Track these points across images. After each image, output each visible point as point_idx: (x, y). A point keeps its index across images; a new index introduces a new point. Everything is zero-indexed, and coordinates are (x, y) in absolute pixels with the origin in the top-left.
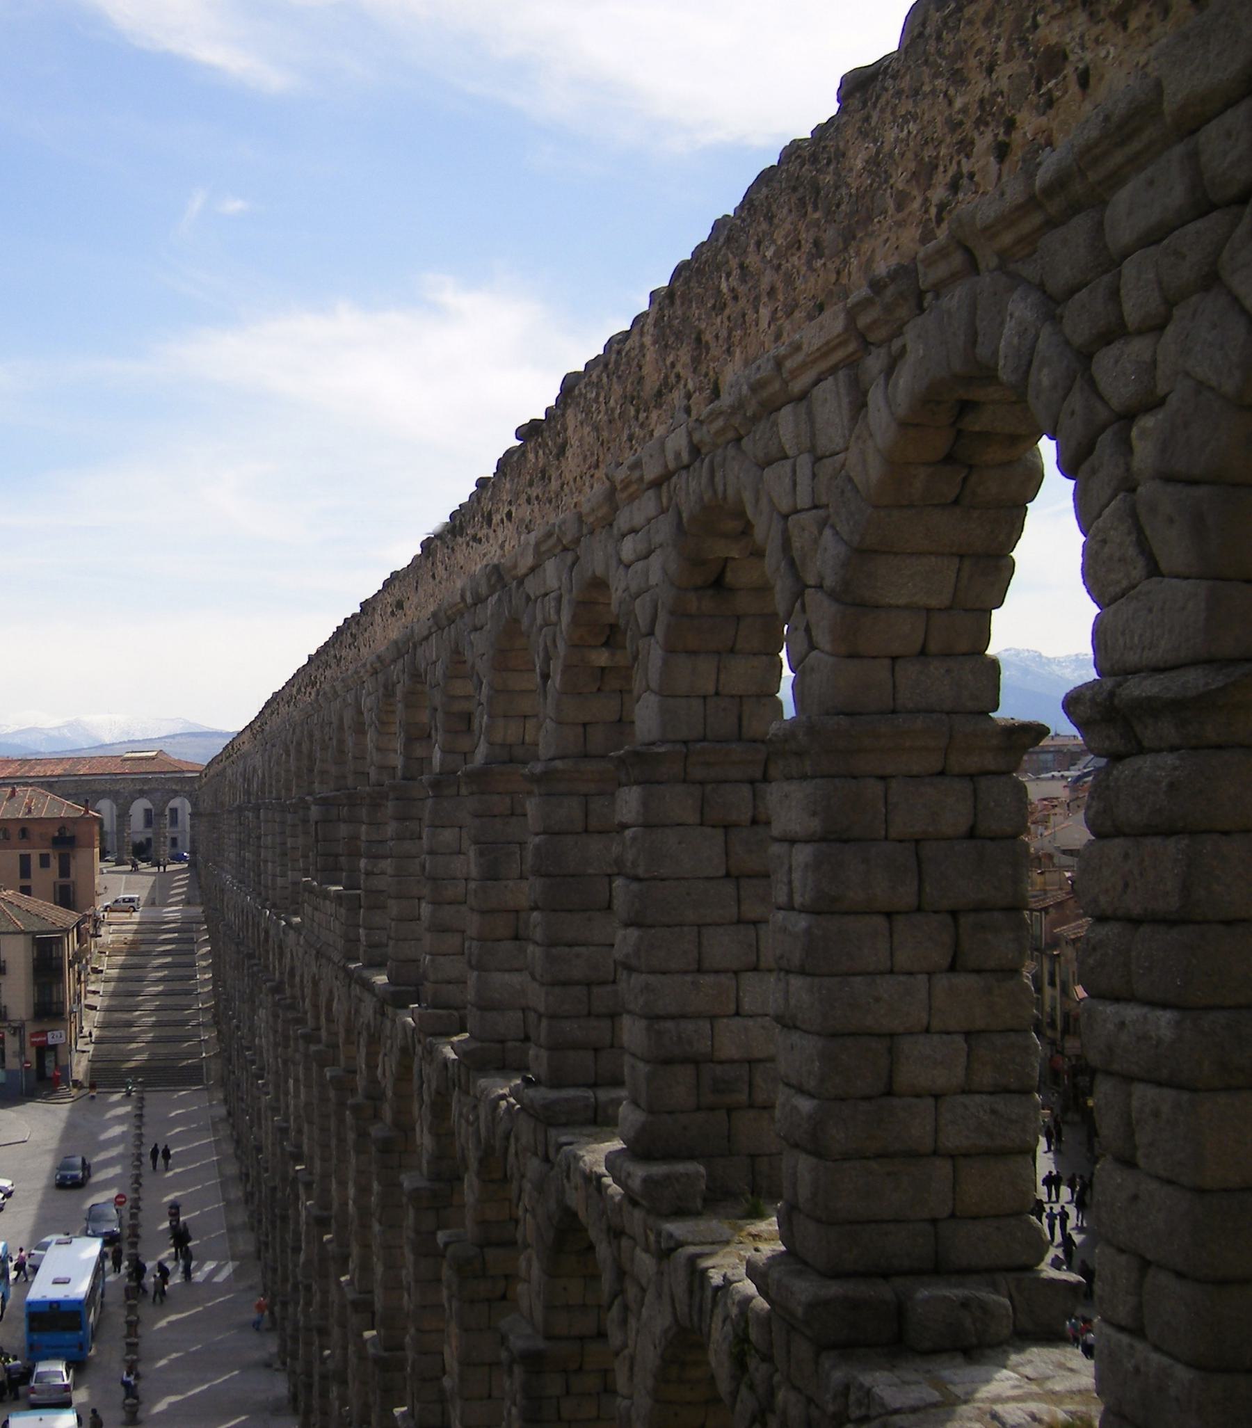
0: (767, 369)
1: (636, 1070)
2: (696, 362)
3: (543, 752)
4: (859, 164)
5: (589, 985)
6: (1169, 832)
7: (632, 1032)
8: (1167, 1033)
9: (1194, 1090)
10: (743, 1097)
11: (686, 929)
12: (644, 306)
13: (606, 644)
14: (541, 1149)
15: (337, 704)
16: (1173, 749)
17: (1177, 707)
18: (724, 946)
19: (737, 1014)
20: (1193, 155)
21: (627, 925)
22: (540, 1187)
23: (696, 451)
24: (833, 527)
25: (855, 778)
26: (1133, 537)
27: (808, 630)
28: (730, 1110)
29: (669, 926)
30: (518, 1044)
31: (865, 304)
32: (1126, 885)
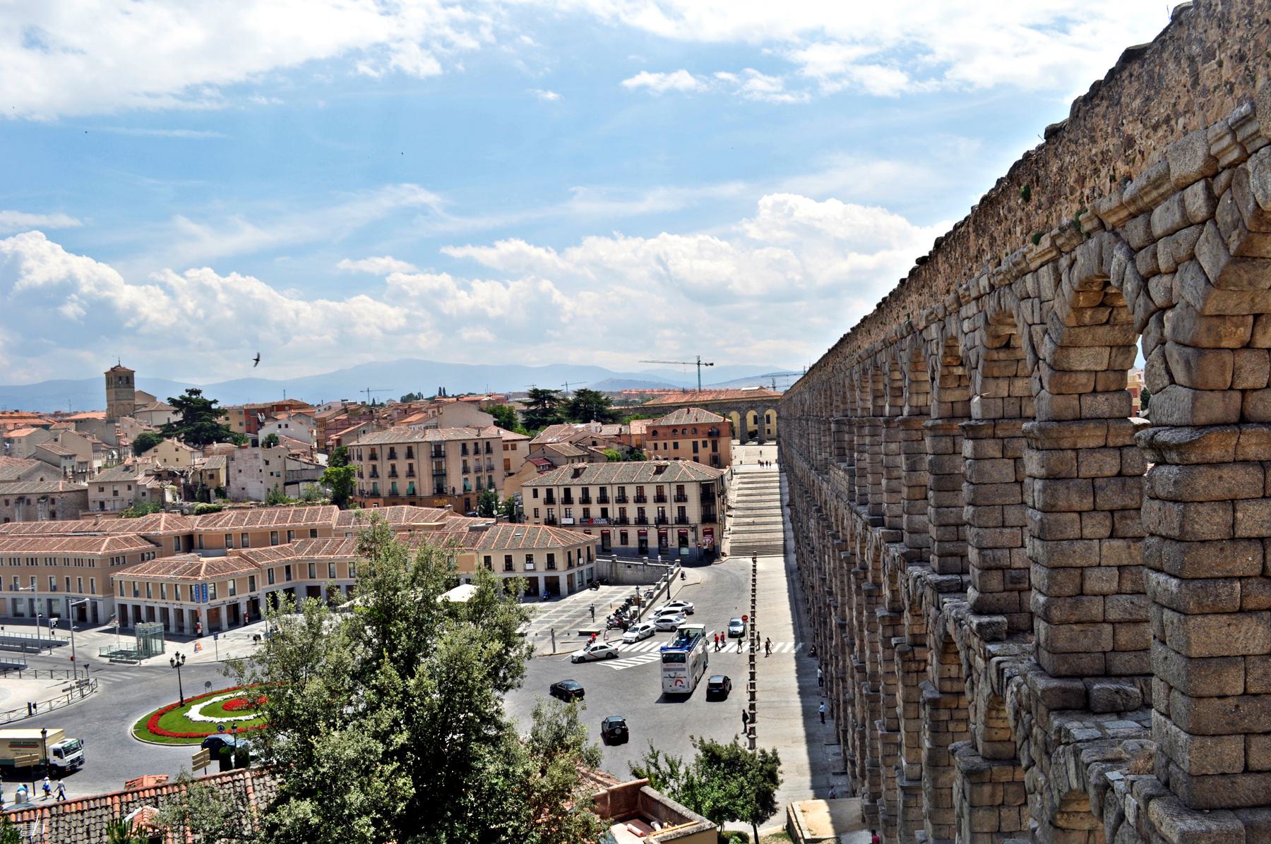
0: (1019, 258)
1: (975, 573)
2: (991, 245)
3: (934, 415)
4: (1055, 170)
6: (1176, 501)
7: (973, 554)
8: (1175, 590)
9: (1186, 615)
12: (969, 212)
15: (842, 375)
16: (1177, 465)
17: (1178, 447)
20: (1182, 201)
21: (969, 504)
22: (935, 621)
23: (992, 287)
28: (1020, 591)
31: (1058, 236)
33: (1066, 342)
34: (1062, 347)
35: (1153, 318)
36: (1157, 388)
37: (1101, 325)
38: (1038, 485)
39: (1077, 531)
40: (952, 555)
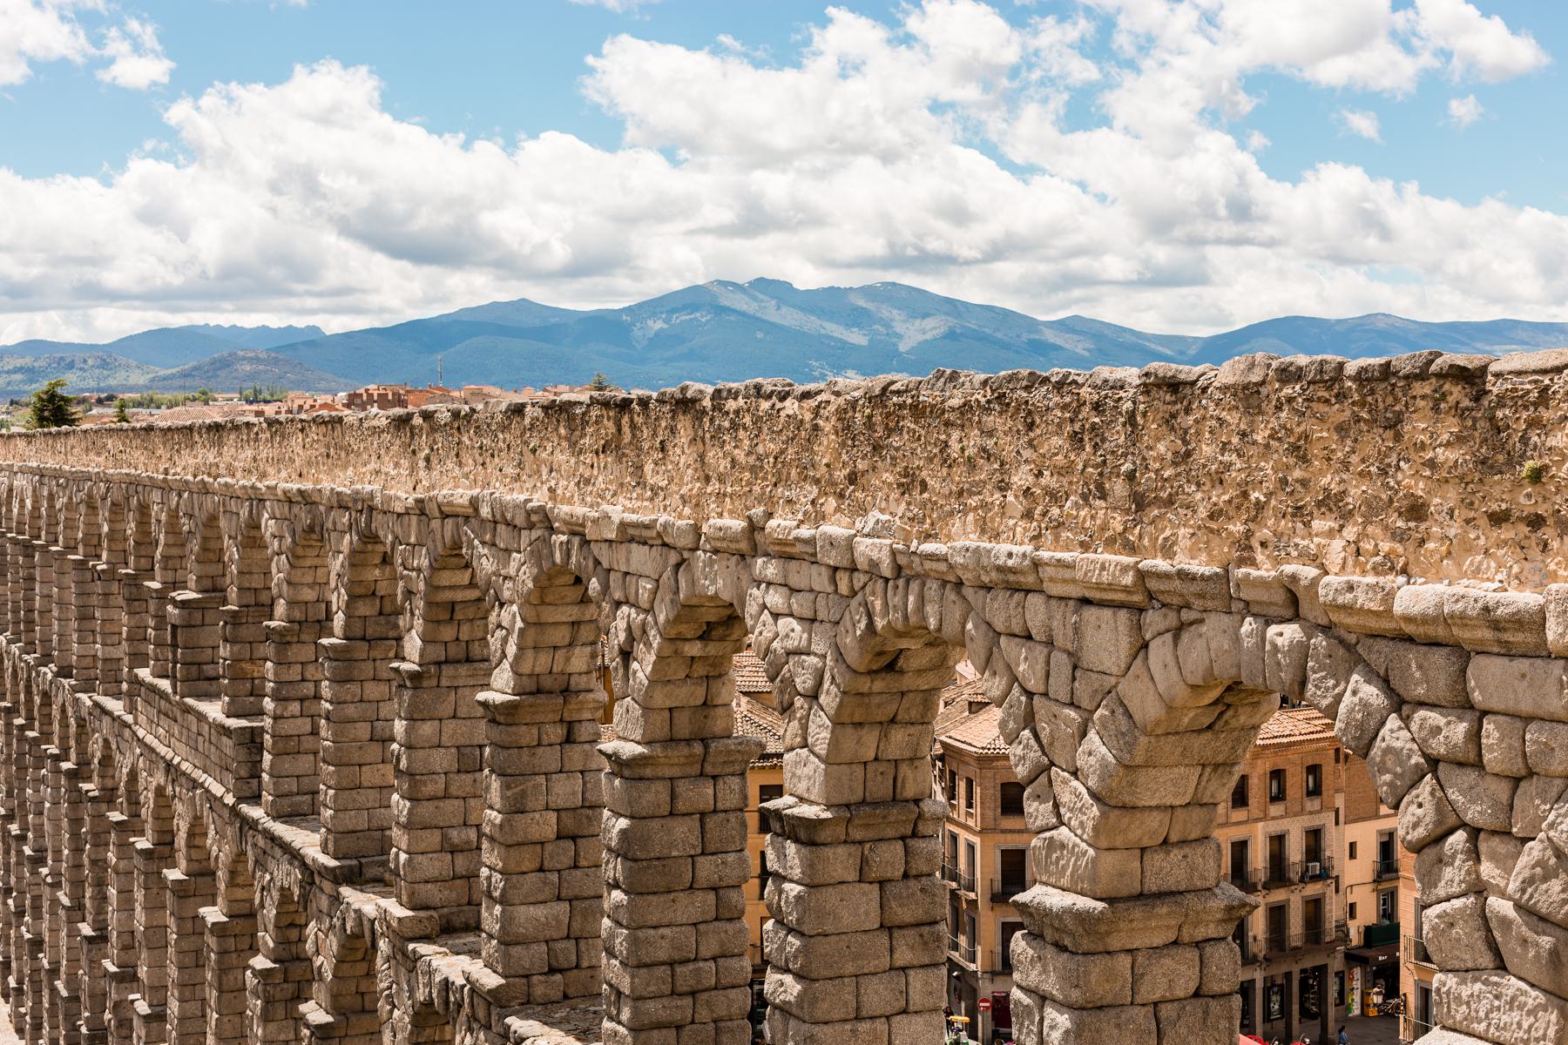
5: (671, 964)
13: (701, 638)
18: (878, 995)
25: (1109, 953)
30: (542, 978)
34: (1127, 767)
40: (660, 1026)
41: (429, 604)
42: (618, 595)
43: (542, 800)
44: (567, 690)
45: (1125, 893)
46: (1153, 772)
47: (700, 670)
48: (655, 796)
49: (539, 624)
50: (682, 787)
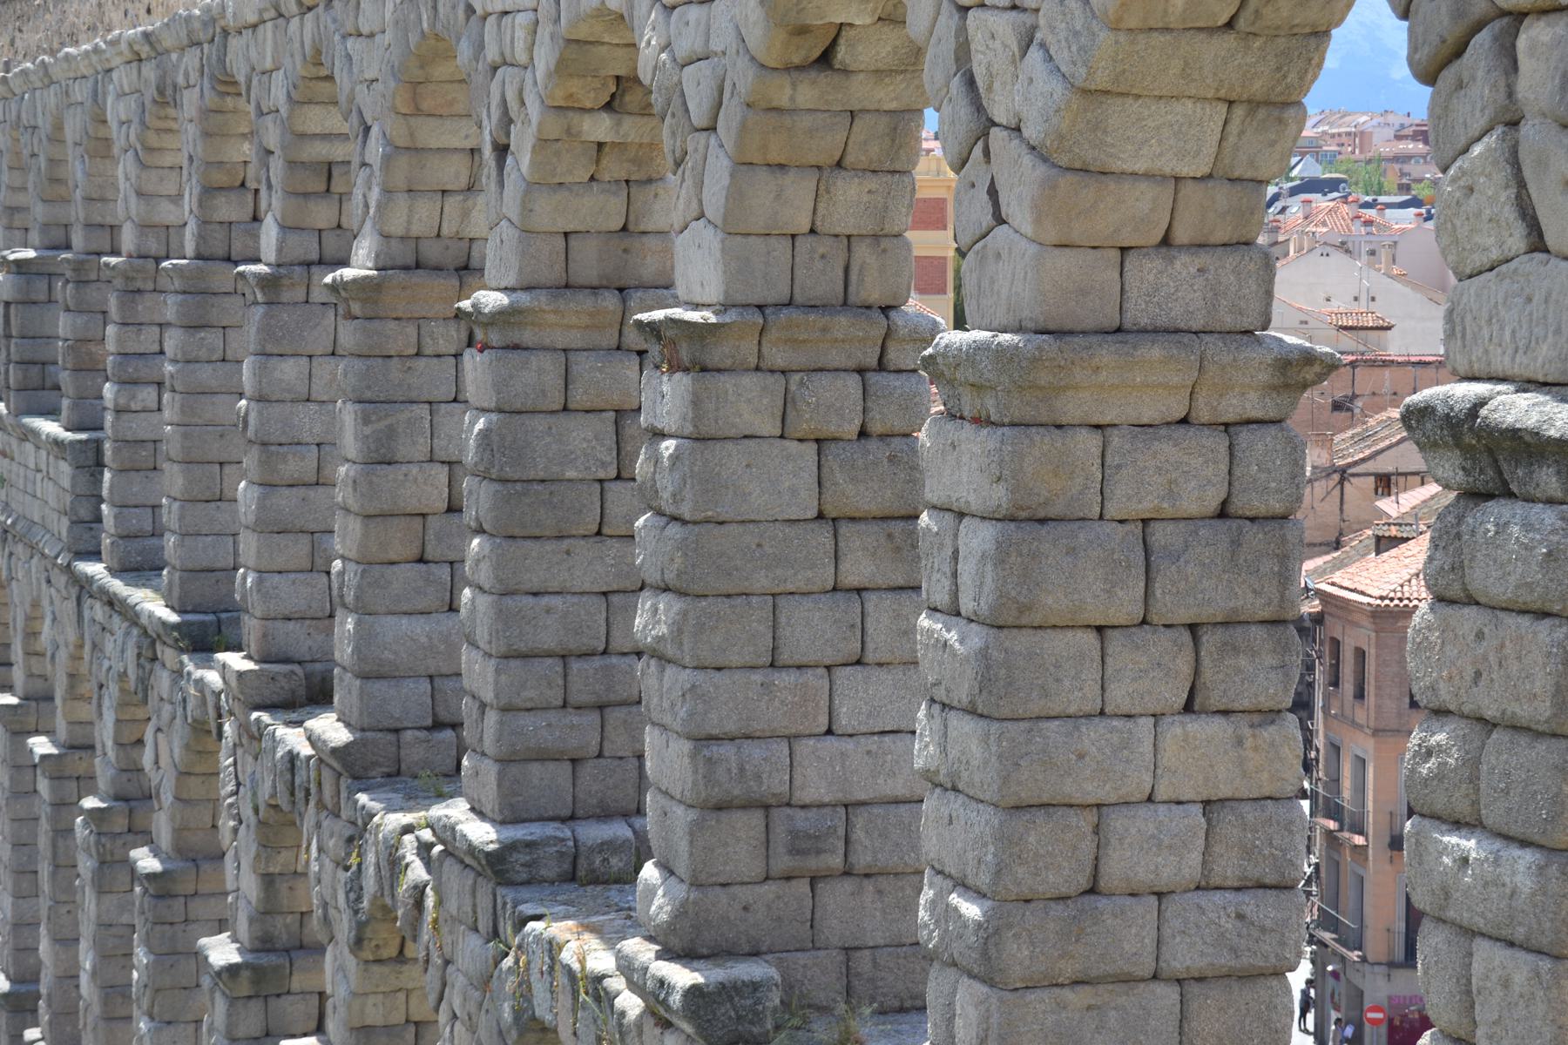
7: (666, 758)
10: (836, 861)
11: (754, 600)
13: (608, 106)
14: (484, 924)
15: (51, 97)
16: (1550, 501)
18: (813, 629)
19: (829, 732)
24: (1042, 45)
25: (1059, 427)
26: (1512, 192)
27: (993, 192)
29: (728, 596)
30: (422, 734)
32: (1478, 674)
33: (1101, 80)
34: (1085, 92)
35: (1483, 38)
36: (1479, 260)
37: (1211, 30)
38: (978, 538)
39: (1092, 689)
40: (543, 756)
41: (292, 164)
42: (491, 54)
43: (421, 449)
44: (466, 268)
45: (1089, 324)
46: (1133, 106)
47: (613, 168)
48: (540, 375)
49: (414, 150)
50: (583, 365)
